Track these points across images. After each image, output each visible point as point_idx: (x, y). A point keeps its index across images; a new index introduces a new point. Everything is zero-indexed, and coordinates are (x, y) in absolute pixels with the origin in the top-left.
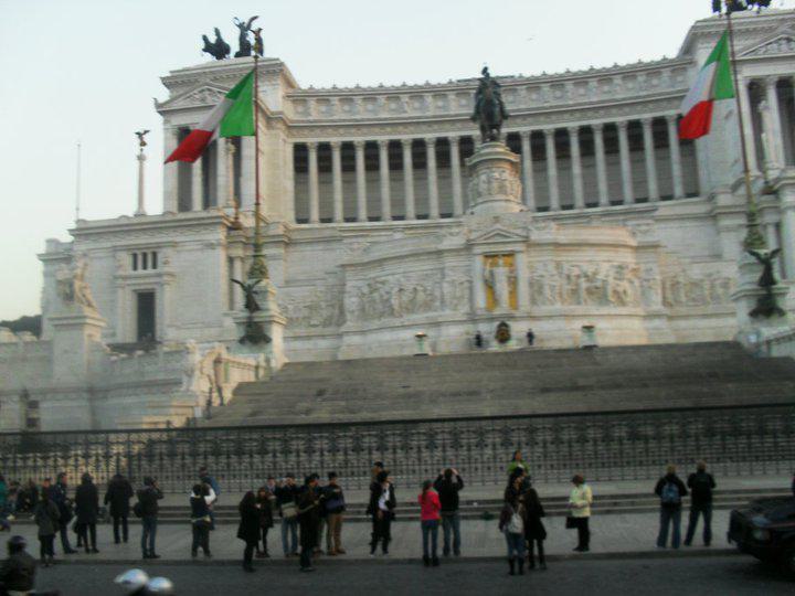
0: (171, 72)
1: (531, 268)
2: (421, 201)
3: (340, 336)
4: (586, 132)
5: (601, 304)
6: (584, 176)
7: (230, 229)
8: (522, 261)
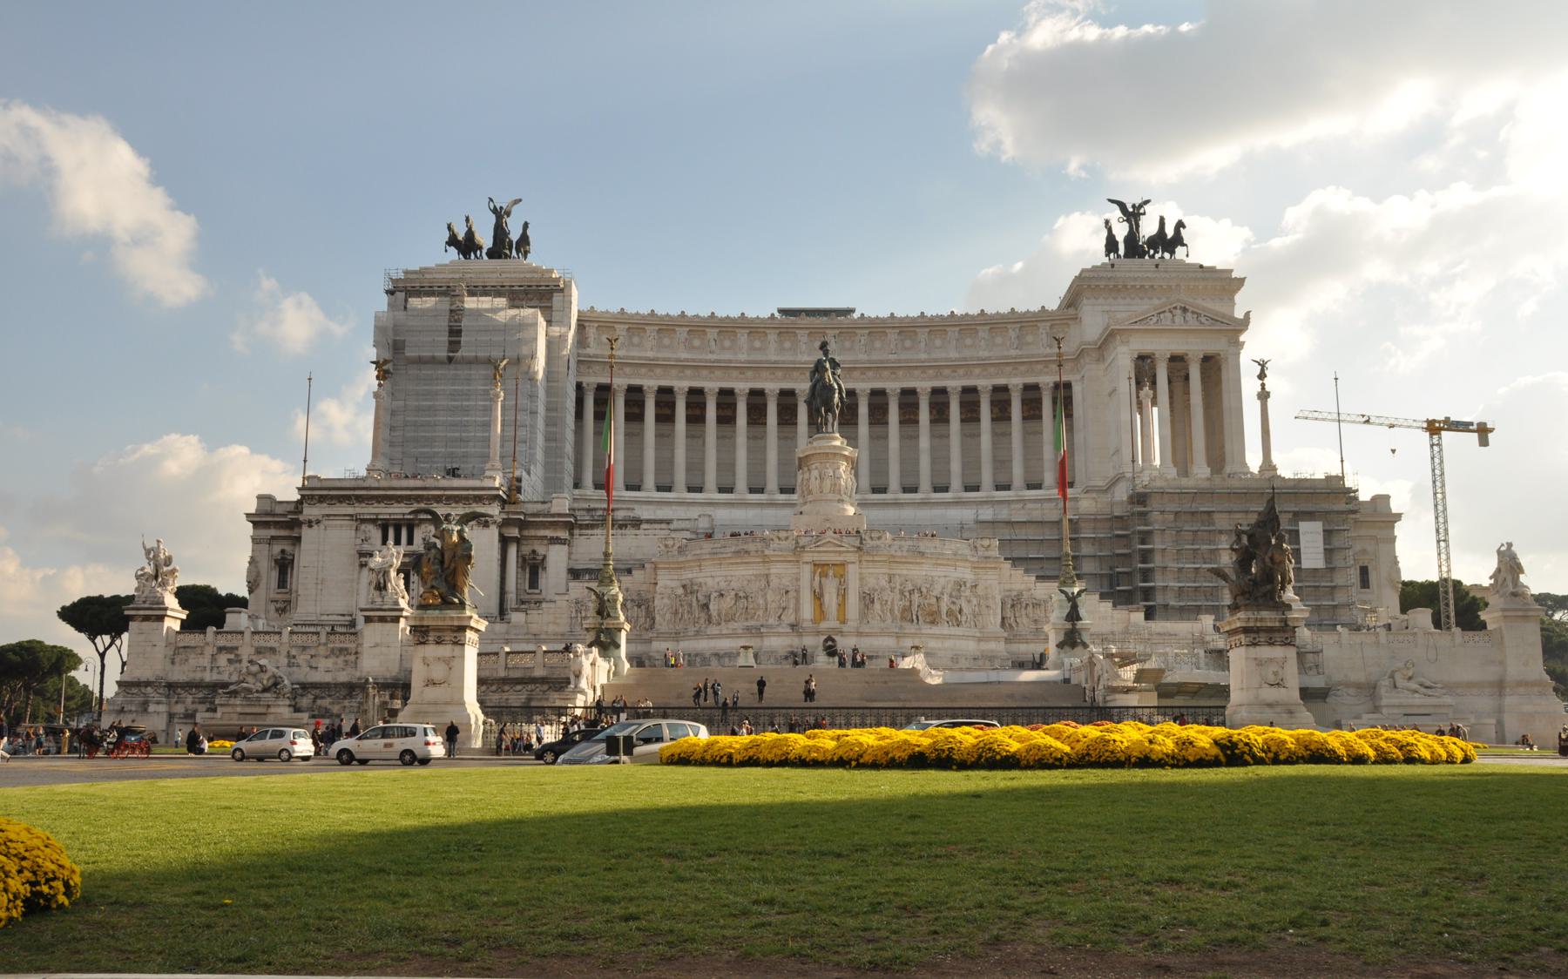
0: (406, 272)
1: (861, 579)
2: (726, 467)
3: (650, 641)
4: (939, 395)
5: (932, 622)
6: (933, 449)
7: (504, 502)
8: (851, 568)
